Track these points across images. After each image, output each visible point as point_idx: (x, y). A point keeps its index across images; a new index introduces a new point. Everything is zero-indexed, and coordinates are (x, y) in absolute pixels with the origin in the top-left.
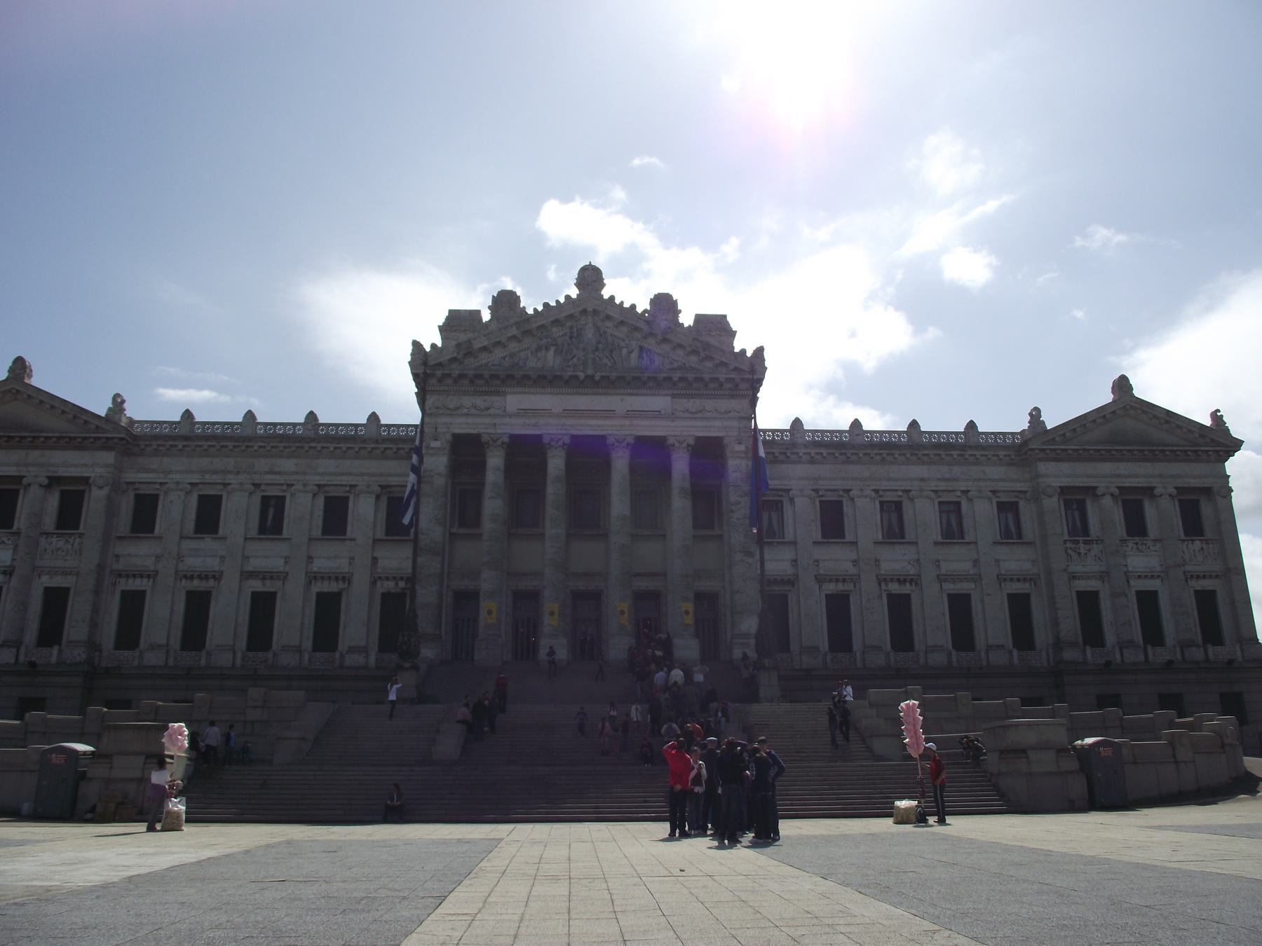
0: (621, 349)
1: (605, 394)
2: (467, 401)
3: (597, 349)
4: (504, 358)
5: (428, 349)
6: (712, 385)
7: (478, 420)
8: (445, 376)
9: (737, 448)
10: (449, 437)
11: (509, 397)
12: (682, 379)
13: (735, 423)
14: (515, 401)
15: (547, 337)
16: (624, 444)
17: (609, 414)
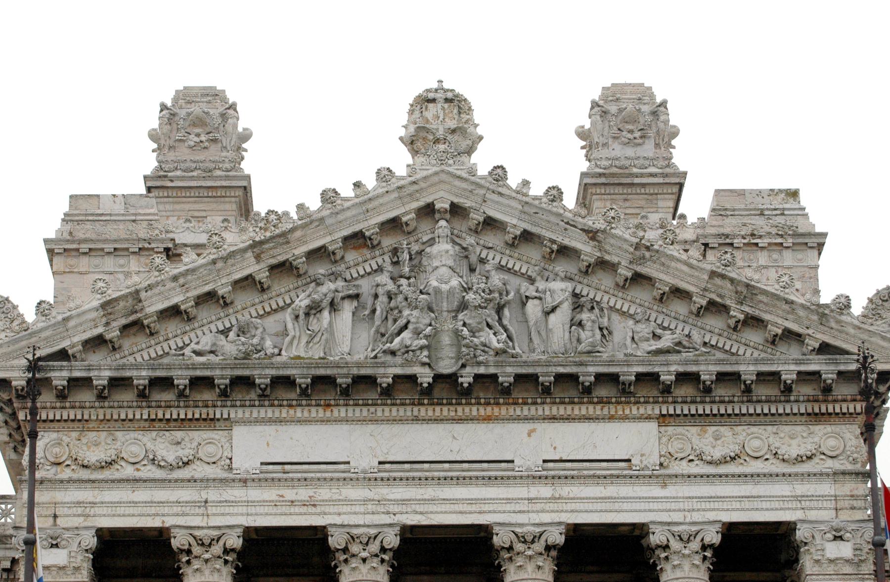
0: (524, 301)
1: (488, 419)
2: (134, 444)
3: (463, 306)
4: (225, 332)
5: (30, 316)
6: (762, 391)
7: (161, 495)
8: (74, 383)
9: (834, 550)
10: (91, 541)
11: (238, 432)
12: (684, 378)
13: (826, 488)
14: (255, 440)
15: (334, 276)
16: (539, 547)
17: (496, 470)
